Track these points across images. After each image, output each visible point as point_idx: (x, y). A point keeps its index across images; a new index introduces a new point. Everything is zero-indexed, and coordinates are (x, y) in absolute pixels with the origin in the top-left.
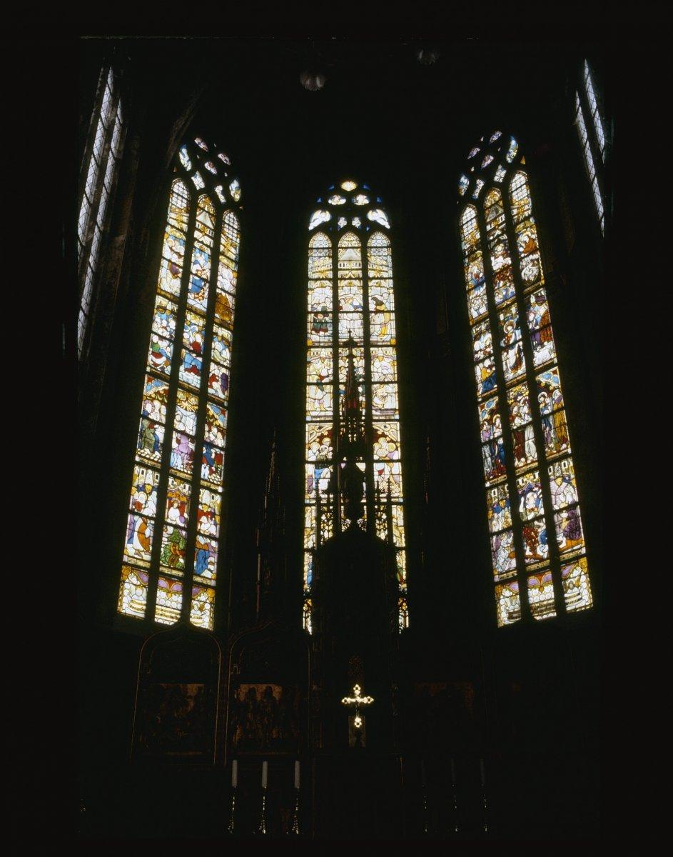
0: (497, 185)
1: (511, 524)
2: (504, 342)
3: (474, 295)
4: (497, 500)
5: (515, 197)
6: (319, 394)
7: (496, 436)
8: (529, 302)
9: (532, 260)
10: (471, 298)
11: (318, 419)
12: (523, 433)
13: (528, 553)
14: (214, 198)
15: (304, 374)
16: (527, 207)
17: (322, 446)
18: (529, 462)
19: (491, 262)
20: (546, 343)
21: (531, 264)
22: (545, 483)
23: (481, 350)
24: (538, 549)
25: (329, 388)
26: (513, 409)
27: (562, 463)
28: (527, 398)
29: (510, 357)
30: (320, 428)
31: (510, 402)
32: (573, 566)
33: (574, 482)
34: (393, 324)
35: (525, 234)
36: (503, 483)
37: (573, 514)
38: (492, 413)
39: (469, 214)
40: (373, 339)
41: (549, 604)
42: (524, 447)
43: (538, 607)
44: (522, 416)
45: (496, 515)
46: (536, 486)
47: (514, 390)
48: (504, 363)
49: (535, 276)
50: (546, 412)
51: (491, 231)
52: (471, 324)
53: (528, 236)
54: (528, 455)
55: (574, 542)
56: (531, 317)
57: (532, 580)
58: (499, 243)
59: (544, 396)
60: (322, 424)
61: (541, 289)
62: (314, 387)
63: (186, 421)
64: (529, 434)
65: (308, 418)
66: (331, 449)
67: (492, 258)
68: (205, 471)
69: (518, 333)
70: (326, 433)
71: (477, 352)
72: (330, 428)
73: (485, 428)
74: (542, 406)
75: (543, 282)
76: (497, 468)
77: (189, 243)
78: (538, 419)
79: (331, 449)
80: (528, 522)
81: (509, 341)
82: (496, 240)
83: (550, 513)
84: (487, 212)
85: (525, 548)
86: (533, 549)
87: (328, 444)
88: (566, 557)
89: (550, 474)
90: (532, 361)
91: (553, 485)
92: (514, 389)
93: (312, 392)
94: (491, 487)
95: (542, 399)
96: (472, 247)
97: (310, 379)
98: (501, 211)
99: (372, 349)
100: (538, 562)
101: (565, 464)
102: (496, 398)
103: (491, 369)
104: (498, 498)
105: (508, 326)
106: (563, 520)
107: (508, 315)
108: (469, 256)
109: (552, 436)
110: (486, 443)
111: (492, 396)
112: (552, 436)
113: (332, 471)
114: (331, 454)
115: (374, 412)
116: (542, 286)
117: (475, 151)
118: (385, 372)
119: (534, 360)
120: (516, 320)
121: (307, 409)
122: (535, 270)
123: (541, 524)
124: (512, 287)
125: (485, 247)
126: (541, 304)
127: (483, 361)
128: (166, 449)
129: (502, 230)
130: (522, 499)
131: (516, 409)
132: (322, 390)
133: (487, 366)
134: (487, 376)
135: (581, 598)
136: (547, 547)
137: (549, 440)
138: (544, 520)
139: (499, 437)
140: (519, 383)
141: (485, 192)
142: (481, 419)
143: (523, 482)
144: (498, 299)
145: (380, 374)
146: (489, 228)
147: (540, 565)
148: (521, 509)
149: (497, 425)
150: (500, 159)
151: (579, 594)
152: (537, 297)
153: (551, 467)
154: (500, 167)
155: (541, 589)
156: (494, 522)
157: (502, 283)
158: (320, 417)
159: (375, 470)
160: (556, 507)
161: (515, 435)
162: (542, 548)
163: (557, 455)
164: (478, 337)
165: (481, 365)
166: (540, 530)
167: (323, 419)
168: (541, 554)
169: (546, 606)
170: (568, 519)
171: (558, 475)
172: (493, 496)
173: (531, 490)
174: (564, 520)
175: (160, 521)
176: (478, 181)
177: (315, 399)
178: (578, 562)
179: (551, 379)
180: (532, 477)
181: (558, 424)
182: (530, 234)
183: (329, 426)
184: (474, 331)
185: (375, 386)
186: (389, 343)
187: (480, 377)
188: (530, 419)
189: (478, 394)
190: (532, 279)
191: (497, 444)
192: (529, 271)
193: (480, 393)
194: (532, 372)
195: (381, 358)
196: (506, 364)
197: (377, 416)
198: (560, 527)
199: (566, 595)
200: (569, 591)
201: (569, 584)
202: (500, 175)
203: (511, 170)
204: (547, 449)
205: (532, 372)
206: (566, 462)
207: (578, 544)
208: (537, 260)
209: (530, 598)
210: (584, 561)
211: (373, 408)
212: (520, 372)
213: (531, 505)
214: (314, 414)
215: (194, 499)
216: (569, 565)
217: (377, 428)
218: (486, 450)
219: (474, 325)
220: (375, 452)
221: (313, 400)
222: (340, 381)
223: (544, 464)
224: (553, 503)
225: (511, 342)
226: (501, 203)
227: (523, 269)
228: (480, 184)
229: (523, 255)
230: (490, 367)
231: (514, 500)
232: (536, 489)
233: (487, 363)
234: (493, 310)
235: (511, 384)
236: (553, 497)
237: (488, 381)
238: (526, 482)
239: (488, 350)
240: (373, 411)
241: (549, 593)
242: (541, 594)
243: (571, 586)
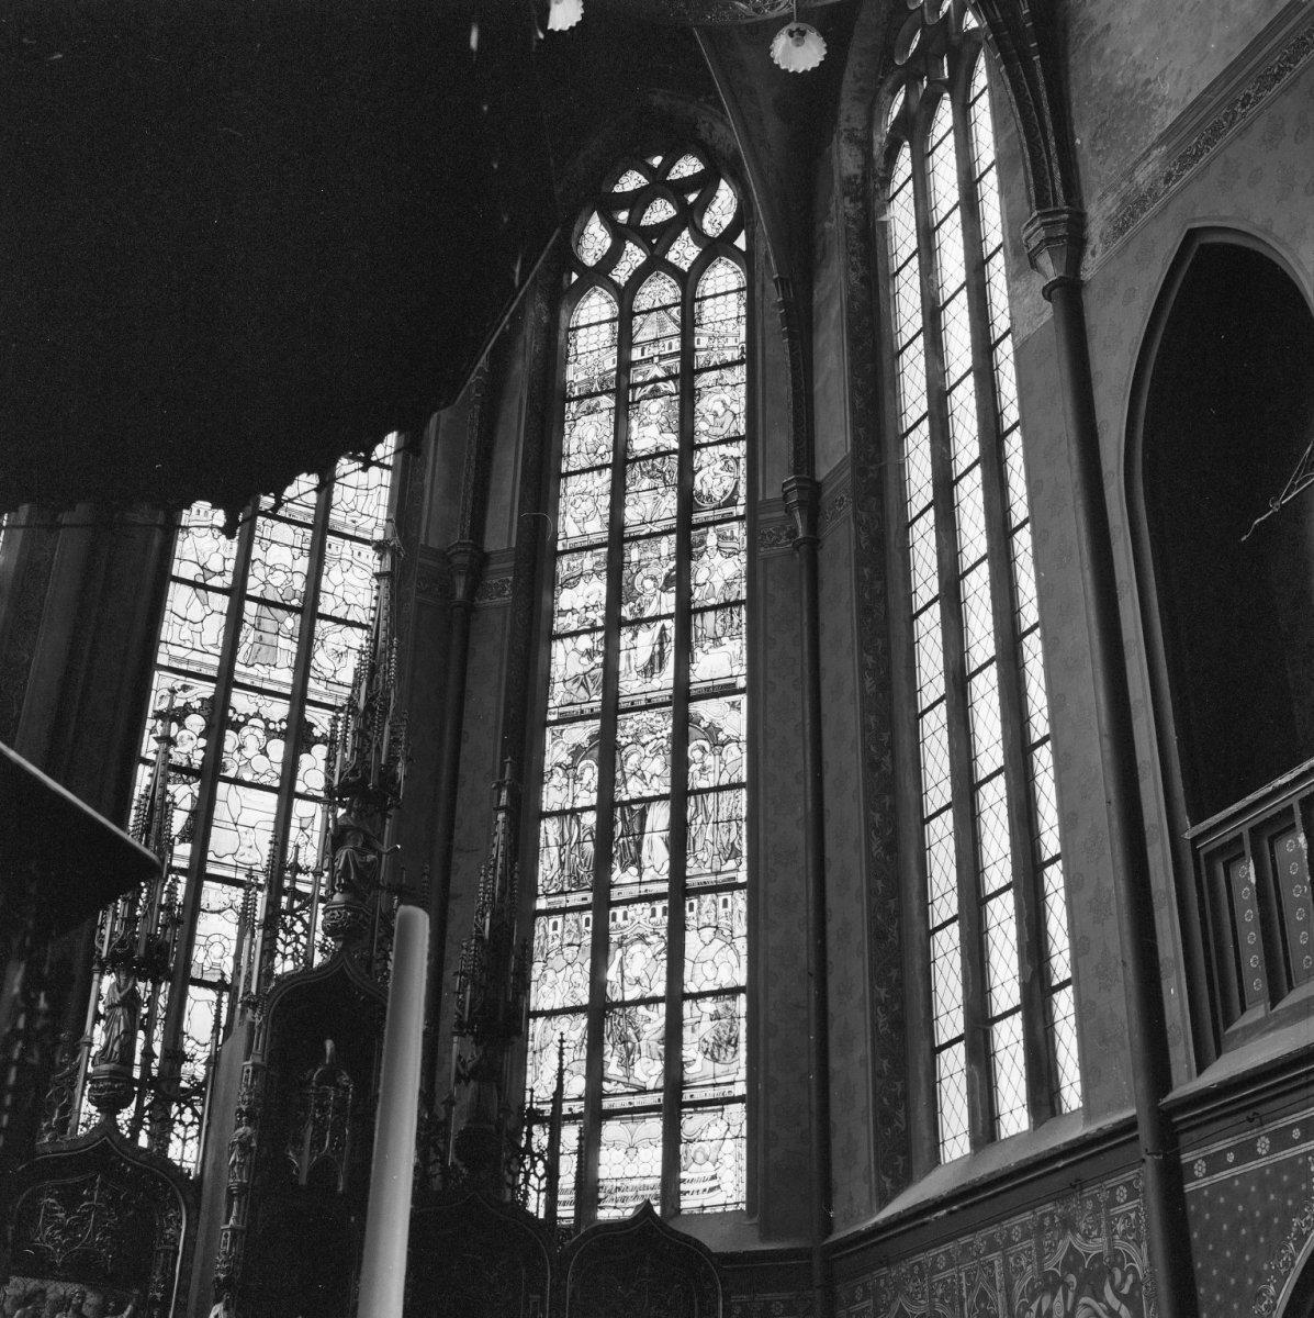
0: (673, 271)
1: (586, 1000)
2: (631, 610)
3: (578, 489)
4: (557, 942)
5: (709, 311)
6: (196, 612)
7: (579, 804)
8: (703, 542)
9: (723, 457)
10: (569, 491)
11: (184, 667)
12: (643, 815)
13: (613, 1068)
15: (167, 553)
16: (731, 342)
17: (183, 732)
18: (645, 878)
19: (628, 430)
20: (725, 640)
21: (721, 464)
23: (572, 610)
24: (637, 1066)
25: (221, 602)
26: (627, 757)
27: (721, 899)
28: (665, 742)
29: (638, 647)
30: (185, 688)
31: (623, 741)
32: (709, 1117)
33: (742, 945)
34: (385, 493)
35: (717, 397)
36: (580, 909)
37: (727, 1008)
38: (577, 752)
39: (596, 307)
40: (336, 517)
41: (645, 1188)
42: (639, 846)
43: (618, 1189)
44: (646, 772)
45: (550, 974)
46: (655, 933)
47: (636, 718)
48: (623, 655)
49: (725, 492)
50: (702, 784)
51: (640, 362)
52: (560, 547)
53: (724, 404)
54: (646, 862)
55: (719, 1068)
56: (701, 576)
57: (611, 1130)
58: (655, 394)
59: (703, 749)
60: (191, 681)
61: (735, 523)
62: (187, 590)
64: (659, 817)
65: (162, 659)
66: (203, 742)
67: (634, 423)
69: (668, 602)
70: (197, 705)
71: (563, 613)
72: (208, 695)
73: (555, 780)
74: (693, 768)
75: (740, 510)
76: (570, 876)
78: (680, 794)
79: (203, 742)
80: (624, 1004)
81: (641, 610)
82: (651, 386)
83: (676, 997)
84: (638, 319)
85: (607, 1058)
86: (627, 1062)
87: (198, 730)
88: (699, 1095)
89: (688, 914)
90: (689, 668)
91: (692, 940)
92: (637, 716)
93: (179, 598)
94: (548, 913)
95: (697, 754)
96: (590, 382)
97: (179, 569)
98: (673, 329)
99: (330, 539)
100: (633, 1094)
101: (725, 901)
102: (594, 725)
103: (591, 659)
104: (562, 939)
105: (646, 578)
106: (700, 1022)
107: (650, 554)
108: (580, 399)
109: (709, 837)
110: (551, 814)
111: (583, 717)
112: (709, 837)
113: (197, 794)
114: (200, 754)
115: (312, 683)
116: (738, 518)
117: (632, 181)
118: (350, 599)
119: (693, 666)
120: (666, 571)
121: (163, 638)
122: (728, 484)
123: (653, 1015)
124: (668, 497)
125: (623, 393)
126: (729, 555)
127: (576, 634)
129: (667, 369)
130: (619, 953)
131: (633, 759)
132: (205, 604)
133: (582, 649)
134: (580, 670)
135: (719, 1187)
136: (659, 1066)
137: (699, 846)
138: (662, 1007)
139: (585, 809)
140: (650, 706)
141: (640, 276)
142: (548, 760)
143: (625, 918)
144: (631, 514)
145: (339, 601)
146: (636, 355)
147: (638, 1101)
148: (612, 974)
149: (585, 781)
150: (688, 218)
151: (714, 1177)
152: (722, 537)
153: (695, 901)
154: (686, 234)
155: (633, 1151)
156: (545, 989)
157: (646, 483)
158: (188, 662)
159: (294, 815)
160: (690, 988)
161: (623, 813)
162: (646, 1067)
163: (713, 878)
164: (571, 582)
165: (568, 641)
166: (647, 1027)
167: (193, 669)
168: (643, 1078)
169: (636, 1189)
170: (716, 1017)
171: (707, 921)
172: (551, 932)
173: (642, 938)
174: (706, 1017)
176: (630, 246)
177: (185, 619)
178: (723, 1110)
179: (729, 718)
180: (648, 912)
181: (723, 815)
182: (728, 402)
183: (207, 690)
184: (565, 563)
185: (321, 625)
186: (368, 537)
187: (561, 669)
188: (667, 790)
189: (551, 704)
190: (717, 494)
191: (579, 823)
192: (718, 474)
193: (557, 703)
194: (683, 695)
195: (346, 565)
196: (629, 657)
197: (317, 692)
198: (693, 1030)
199: (683, 1175)
200: (694, 1167)
201: (696, 1152)
202: (684, 252)
203: (714, 249)
204: (690, 862)
205: (683, 695)
206: (729, 897)
207: (727, 1073)
208: (737, 460)
209: (600, 1168)
210: (737, 1113)
211: (312, 673)
212: (656, 683)
214: (175, 651)
216: (702, 1112)
217: (313, 721)
218: (550, 829)
219: (565, 552)
220: (300, 775)
221: (181, 622)
222: (248, 592)
223: (679, 893)
224: (687, 976)
225: (647, 614)
226: (675, 312)
227: (700, 469)
228: (634, 256)
229: (704, 440)
230: (590, 654)
232: (653, 939)
233: (585, 642)
234: (617, 537)
235: (633, 703)
236: (688, 964)
237: (581, 681)
238: (633, 920)
239: (591, 615)
240: (311, 680)
241: (650, 1162)
243: (700, 1158)
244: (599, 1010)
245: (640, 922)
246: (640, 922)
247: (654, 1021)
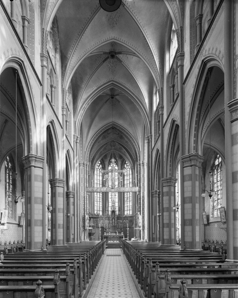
14: (99, 168)
22: (130, 203)
63: (98, 196)
64: (129, 198)
68: (100, 201)
77: (97, 176)
78: (130, 197)
83: (130, 206)
128: (97, 199)
175: (97, 206)
213: (128, 205)
215: (100, 203)
223: (130, 201)
231: (127, 203)
234: (127, 184)
242: (128, 212)
244: (127, 206)
245: (128, 202)
246: (128, 202)
247: (129, 206)
